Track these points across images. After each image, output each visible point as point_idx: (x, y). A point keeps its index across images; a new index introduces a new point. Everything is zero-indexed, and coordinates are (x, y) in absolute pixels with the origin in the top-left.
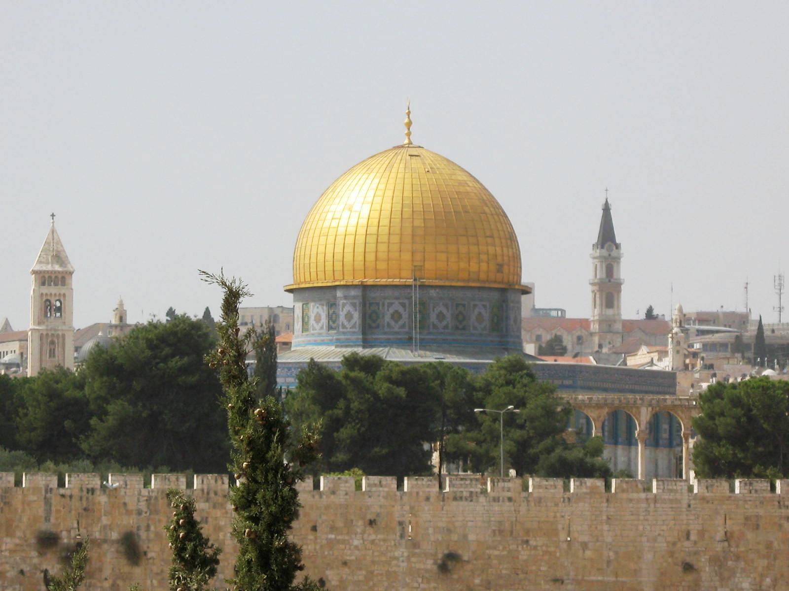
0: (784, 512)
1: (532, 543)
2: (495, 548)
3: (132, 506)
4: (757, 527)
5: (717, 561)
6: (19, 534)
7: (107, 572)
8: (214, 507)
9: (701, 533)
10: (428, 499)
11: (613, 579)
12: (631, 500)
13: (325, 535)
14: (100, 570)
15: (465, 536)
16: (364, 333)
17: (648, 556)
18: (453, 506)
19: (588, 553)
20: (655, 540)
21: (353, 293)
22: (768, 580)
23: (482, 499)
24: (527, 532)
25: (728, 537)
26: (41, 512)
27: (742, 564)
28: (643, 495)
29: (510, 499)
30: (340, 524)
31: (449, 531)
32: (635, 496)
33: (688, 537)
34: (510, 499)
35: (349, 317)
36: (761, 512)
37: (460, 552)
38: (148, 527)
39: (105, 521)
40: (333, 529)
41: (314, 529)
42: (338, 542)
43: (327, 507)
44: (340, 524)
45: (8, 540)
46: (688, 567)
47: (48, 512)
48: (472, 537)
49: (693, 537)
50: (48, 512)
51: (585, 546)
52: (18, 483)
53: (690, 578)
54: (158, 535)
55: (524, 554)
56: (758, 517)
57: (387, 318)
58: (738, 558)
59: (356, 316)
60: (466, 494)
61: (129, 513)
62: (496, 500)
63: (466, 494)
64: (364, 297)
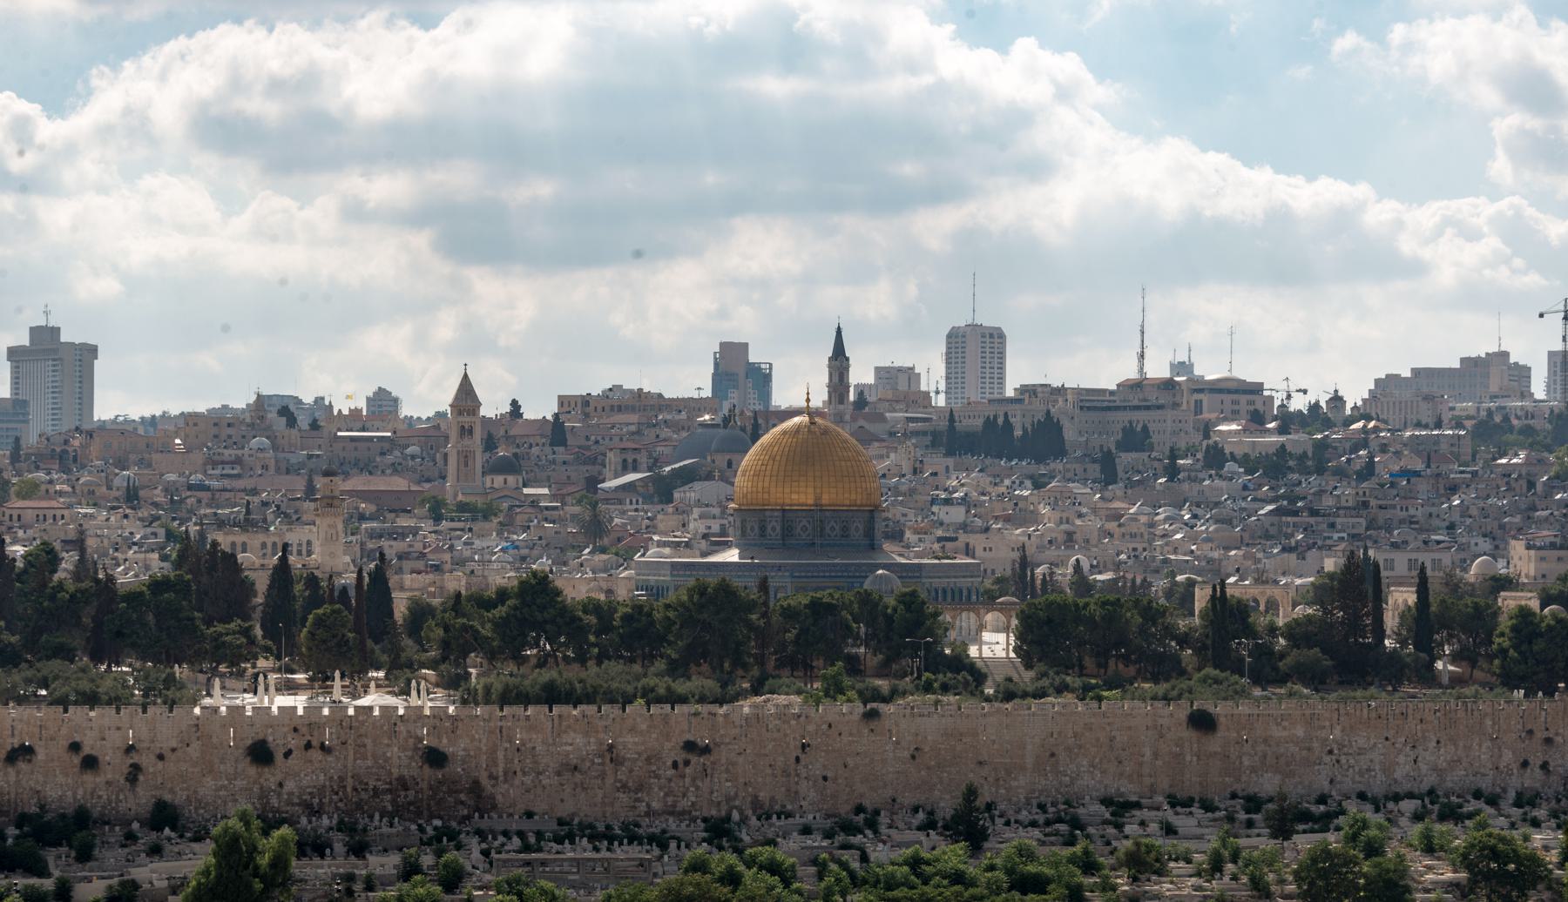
0: (1106, 720)
1: (964, 740)
2: (943, 744)
3: (736, 724)
4: (1091, 729)
5: (1069, 749)
6: (673, 739)
7: (724, 761)
8: (784, 722)
9: (1060, 733)
10: (904, 716)
11: (1008, 761)
12: (1020, 715)
13: (845, 738)
14: (720, 760)
15: (926, 738)
16: (783, 540)
17: (1029, 747)
18: (919, 720)
19: (995, 746)
20: (1033, 737)
21: (776, 514)
22: (1097, 760)
23: (935, 716)
24: (961, 735)
25: (1075, 735)
26: (686, 728)
27: (1082, 751)
28: (1027, 712)
29: (951, 716)
30: (855, 731)
31: (917, 735)
32: (1022, 712)
33: (1052, 736)
34: (951, 716)
35: (774, 529)
36: (1093, 720)
37: (923, 746)
38: (746, 736)
39: (722, 732)
40: (851, 735)
41: (840, 734)
42: (854, 742)
43: (848, 722)
44: (855, 731)
45: (666, 743)
46: (1053, 755)
47: (690, 728)
48: (929, 738)
49: (1055, 736)
50: (690, 728)
51: (994, 741)
52: (673, 709)
53: (1053, 759)
54: (752, 740)
55: (959, 748)
56: (1092, 723)
57: (799, 530)
58: (1080, 747)
59: (778, 528)
60: (926, 713)
61: (735, 727)
62: (943, 716)
63: (926, 713)
64: (784, 516)
